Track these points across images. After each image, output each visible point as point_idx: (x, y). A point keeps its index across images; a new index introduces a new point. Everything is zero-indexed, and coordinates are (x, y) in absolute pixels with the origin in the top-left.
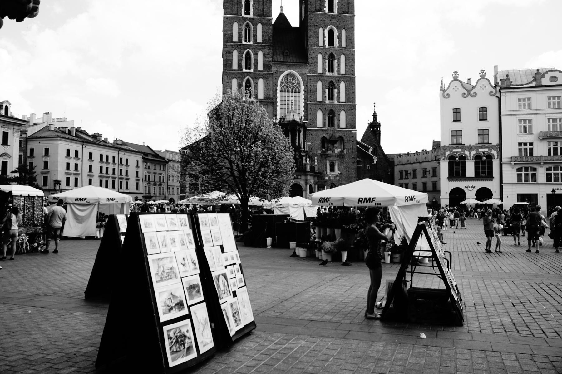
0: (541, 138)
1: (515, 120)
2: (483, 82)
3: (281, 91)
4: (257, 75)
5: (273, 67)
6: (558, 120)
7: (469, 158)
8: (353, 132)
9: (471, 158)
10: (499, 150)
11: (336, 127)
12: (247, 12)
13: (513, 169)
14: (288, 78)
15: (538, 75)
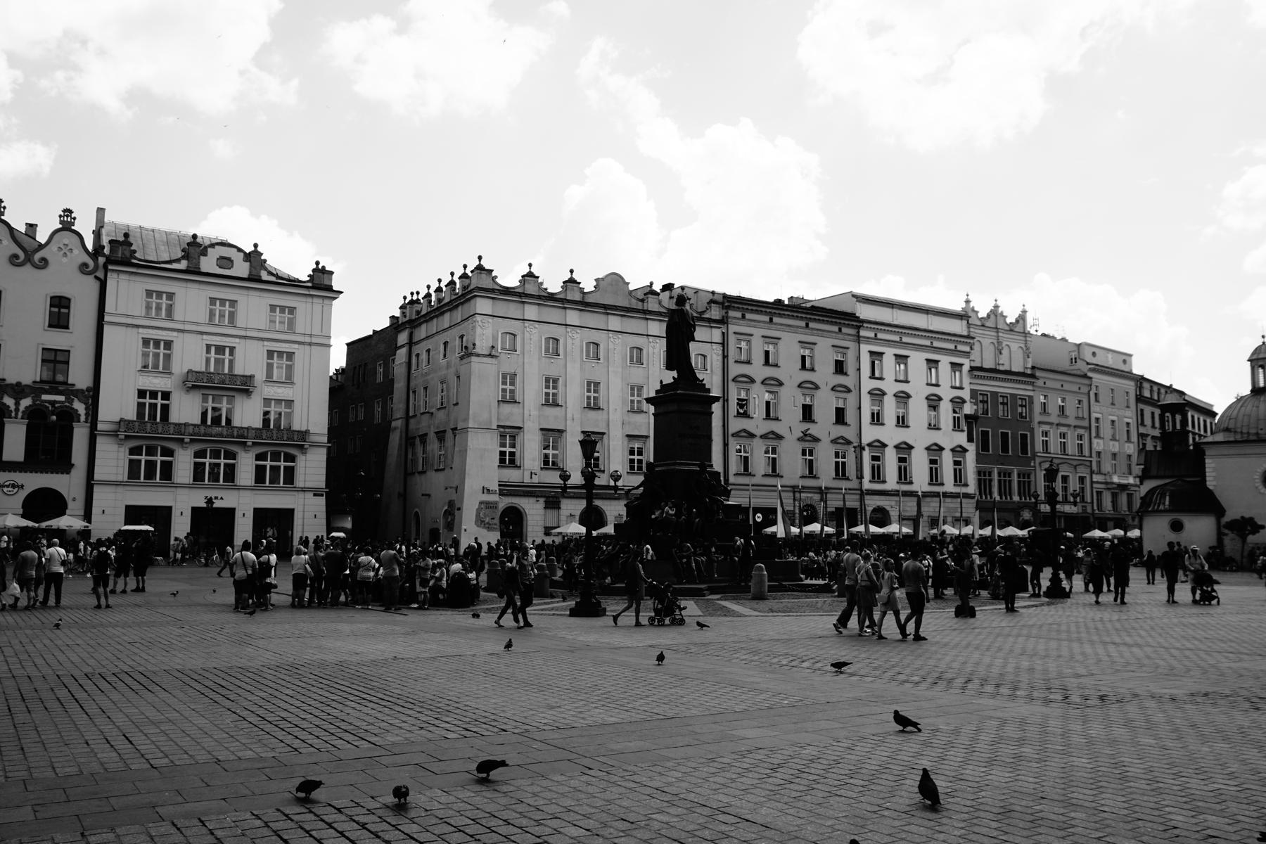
0: (190, 384)
1: (135, 337)
2: (66, 238)
6: (227, 350)
7: (13, 415)
9: (20, 415)
10: (90, 401)
13: (122, 449)
15: (194, 248)
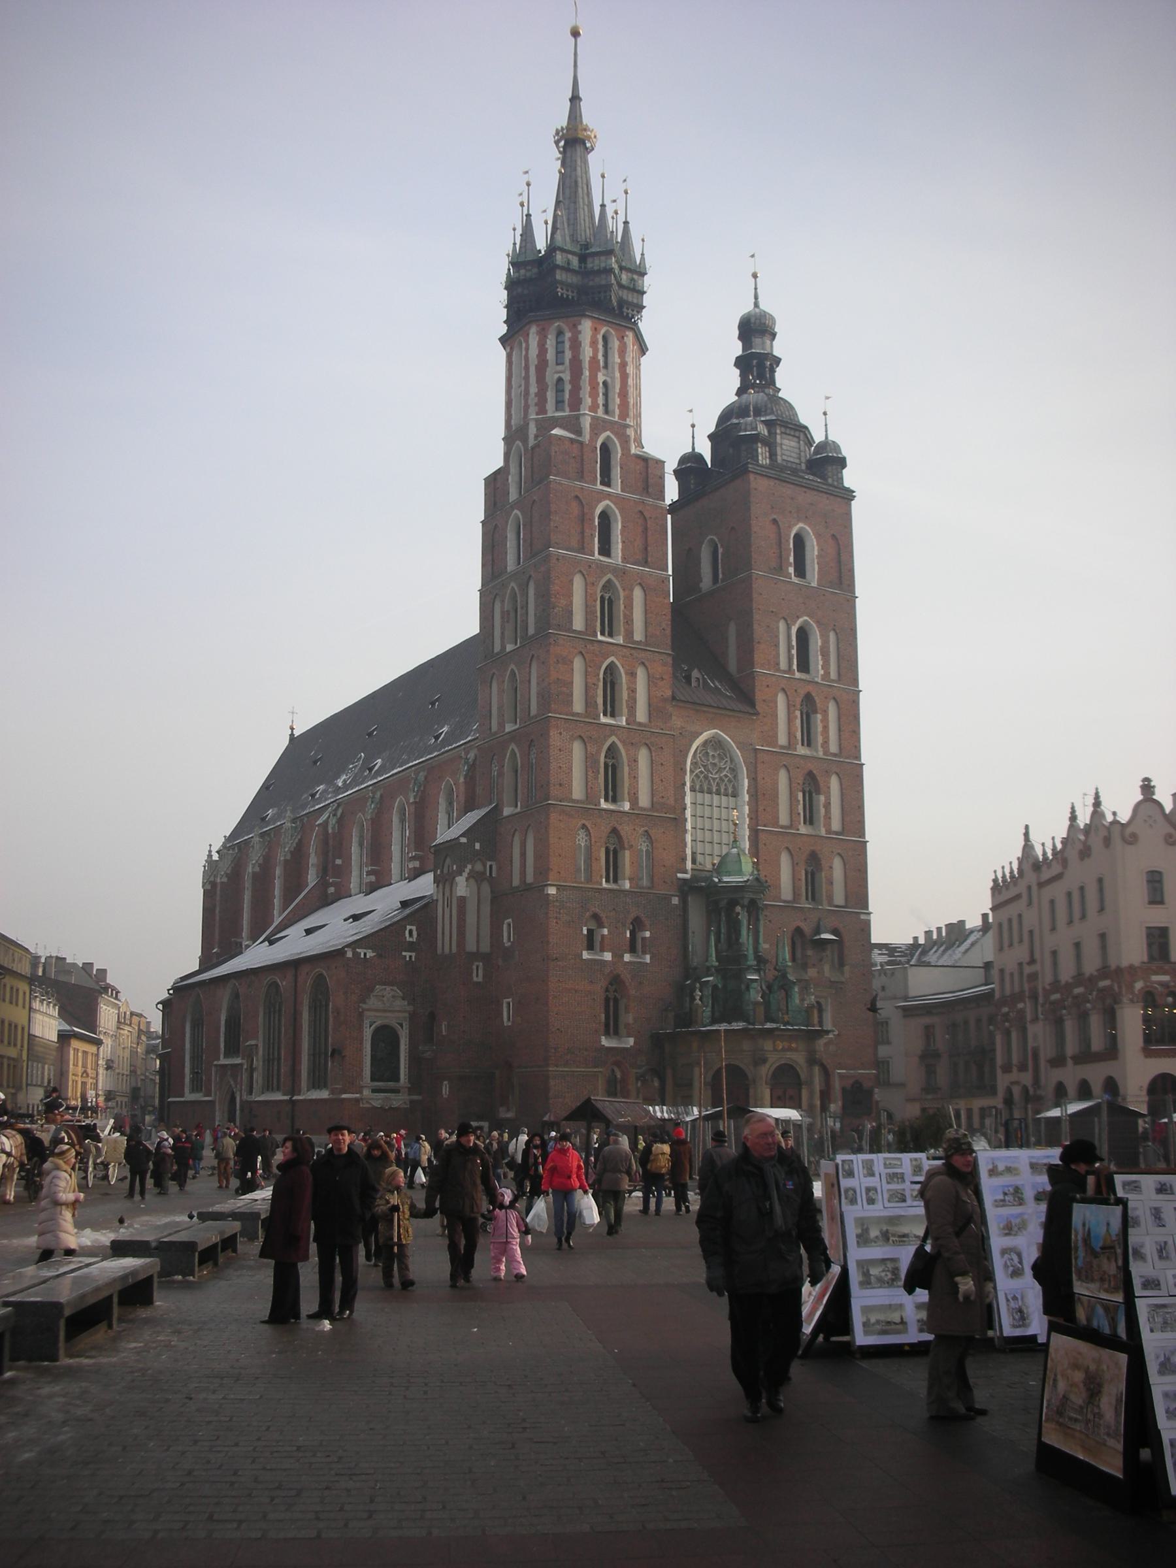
3: (693, 789)
4: (636, 735)
5: (674, 718)
8: (863, 917)
11: (825, 902)
12: (605, 550)
14: (707, 753)
